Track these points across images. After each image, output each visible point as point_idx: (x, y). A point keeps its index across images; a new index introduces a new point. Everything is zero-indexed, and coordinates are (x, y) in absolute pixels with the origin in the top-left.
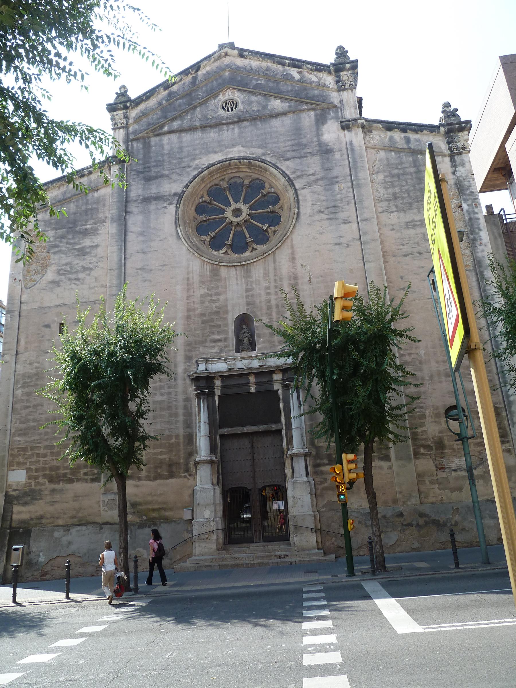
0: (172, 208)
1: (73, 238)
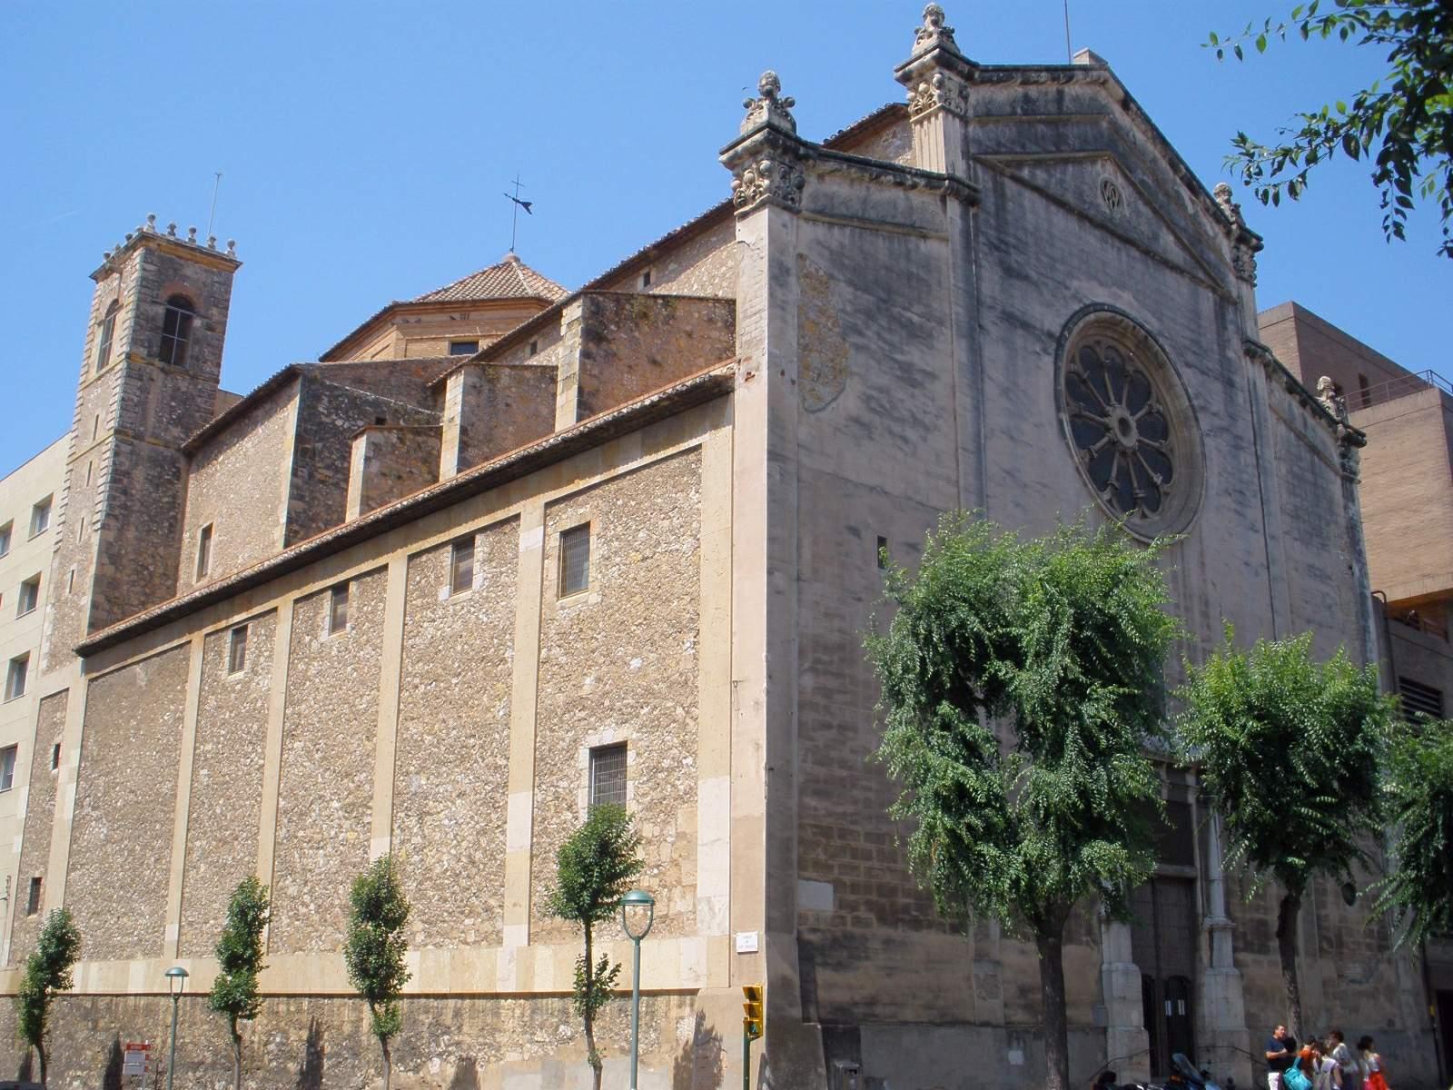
0: (1048, 361)
1: (890, 330)
